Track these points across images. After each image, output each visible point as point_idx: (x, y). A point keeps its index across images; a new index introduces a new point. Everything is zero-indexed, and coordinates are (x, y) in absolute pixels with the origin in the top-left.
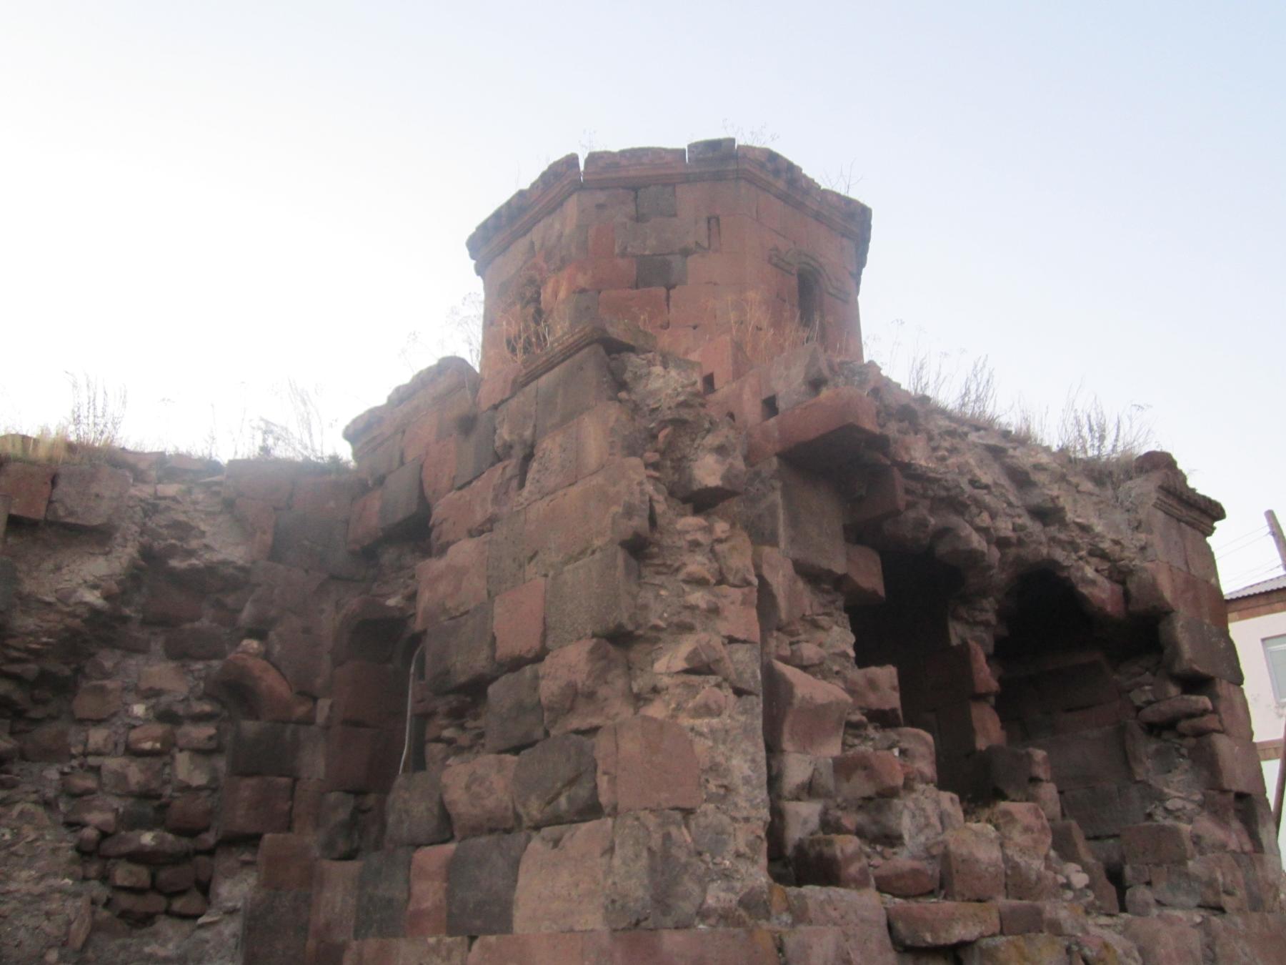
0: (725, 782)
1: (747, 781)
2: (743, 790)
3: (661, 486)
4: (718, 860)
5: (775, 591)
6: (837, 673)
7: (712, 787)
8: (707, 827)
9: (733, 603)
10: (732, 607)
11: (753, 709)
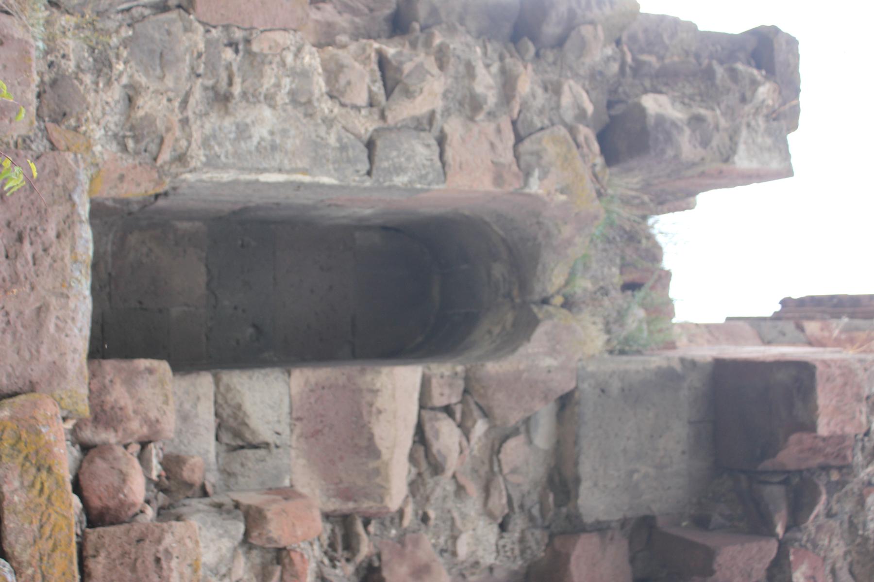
0: (237, 90)
1: (242, 131)
2: (228, 122)
3: (615, 67)
4: (125, 53)
5: (522, 350)
6: (425, 519)
7: (228, 54)
8: (169, 33)
9: (492, 146)
10: (486, 146)
11: (349, 161)
